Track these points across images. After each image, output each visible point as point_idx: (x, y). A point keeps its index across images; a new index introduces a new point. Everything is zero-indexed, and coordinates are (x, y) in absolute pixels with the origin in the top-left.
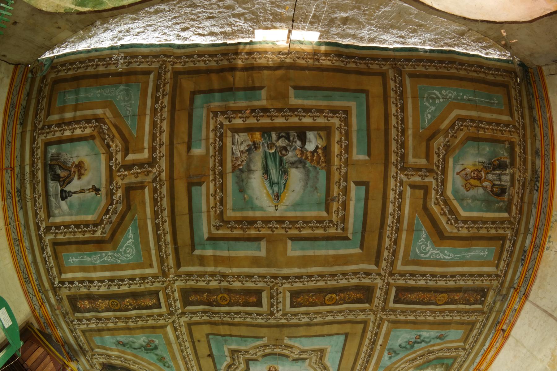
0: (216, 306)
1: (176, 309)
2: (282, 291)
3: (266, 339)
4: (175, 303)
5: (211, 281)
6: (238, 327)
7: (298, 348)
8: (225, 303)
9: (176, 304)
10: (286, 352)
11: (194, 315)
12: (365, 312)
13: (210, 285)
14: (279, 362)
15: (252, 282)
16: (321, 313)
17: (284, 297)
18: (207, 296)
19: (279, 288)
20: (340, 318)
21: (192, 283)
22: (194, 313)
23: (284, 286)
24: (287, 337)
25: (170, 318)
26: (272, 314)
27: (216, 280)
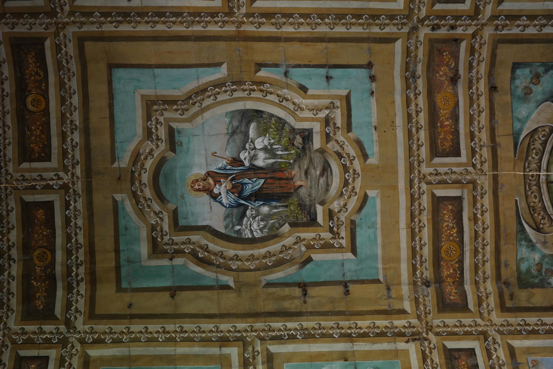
0: (54, 268)
1: (57, 333)
2: (20, 174)
3: (118, 197)
4: (45, 333)
5: (9, 273)
6: (96, 240)
7: (141, 143)
8: (49, 254)
9: (48, 331)
10: (149, 164)
11: (72, 305)
12: (60, 44)
13: (15, 275)
14: (178, 175)
15: (8, 215)
16: (63, 115)
17: (31, 170)
18: (35, 279)
19: (14, 178)
20: (74, 84)
21: (14, 301)
22: (68, 305)
23: (11, 170)
24: (113, 162)
25: (73, 346)
26: (65, 187)
27: (10, 265)
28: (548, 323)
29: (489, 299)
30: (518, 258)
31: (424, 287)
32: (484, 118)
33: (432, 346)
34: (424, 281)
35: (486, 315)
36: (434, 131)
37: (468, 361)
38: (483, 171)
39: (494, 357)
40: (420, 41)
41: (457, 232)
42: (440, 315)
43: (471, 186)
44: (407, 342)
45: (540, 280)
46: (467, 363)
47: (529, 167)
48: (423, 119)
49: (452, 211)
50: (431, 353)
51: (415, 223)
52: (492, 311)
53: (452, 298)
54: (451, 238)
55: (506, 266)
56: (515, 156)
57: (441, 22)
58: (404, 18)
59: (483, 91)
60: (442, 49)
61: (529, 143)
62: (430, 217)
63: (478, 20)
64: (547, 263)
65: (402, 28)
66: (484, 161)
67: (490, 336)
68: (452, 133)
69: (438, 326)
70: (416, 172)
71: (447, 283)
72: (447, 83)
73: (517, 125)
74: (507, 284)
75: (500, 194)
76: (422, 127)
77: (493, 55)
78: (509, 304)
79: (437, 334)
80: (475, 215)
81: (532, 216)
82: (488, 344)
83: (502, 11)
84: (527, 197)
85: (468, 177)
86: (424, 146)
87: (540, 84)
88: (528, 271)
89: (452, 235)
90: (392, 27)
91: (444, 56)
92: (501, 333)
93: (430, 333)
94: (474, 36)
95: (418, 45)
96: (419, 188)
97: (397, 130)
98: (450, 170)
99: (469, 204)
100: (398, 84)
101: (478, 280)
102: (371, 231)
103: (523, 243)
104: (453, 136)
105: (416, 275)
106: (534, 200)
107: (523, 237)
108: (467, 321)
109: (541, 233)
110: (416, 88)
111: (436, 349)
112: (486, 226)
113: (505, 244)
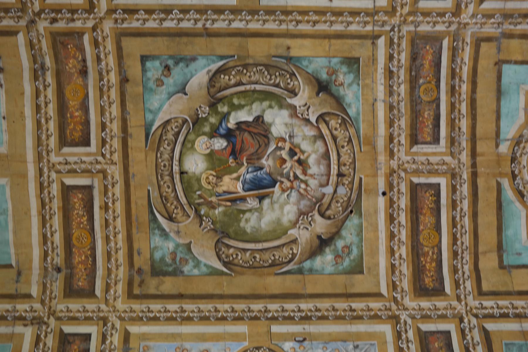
28: (171, 310)
29: (117, 286)
30: (152, 246)
31: (55, 273)
32: (115, 110)
33: (49, 330)
34: (55, 267)
35: (111, 301)
36: (64, 122)
37: (81, 346)
38: (113, 161)
39: (108, 342)
40: (41, 34)
41: (87, 220)
42: (66, 300)
43: (101, 175)
44: (25, 325)
45: (175, 268)
46: (79, 348)
47: (161, 157)
48: (52, 110)
49: (82, 199)
50: (46, 336)
51: (46, 210)
52: (118, 298)
53: (80, 284)
54: (81, 226)
55: (139, 254)
56: (146, 146)
57: (57, 15)
58: (18, 11)
59: (114, 83)
60: (64, 42)
61: (161, 135)
62: (61, 205)
63: (95, 14)
64: (181, 252)
65: (19, 21)
66: (114, 151)
67: (109, 321)
68: (81, 124)
69: (62, 311)
70: (45, 160)
71: (78, 270)
72: (76, 75)
73: (149, 117)
74: (140, 271)
75: (132, 183)
76: (51, 117)
77: (119, 49)
78: (137, 291)
79: (59, 319)
80: (106, 204)
81: (165, 205)
82: (106, 330)
83: (118, 5)
84: (159, 187)
85: (98, 167)
86: (53, 137)
87: (171, 76)
88: (162, 259)
89: (82, 223)
90: (9, 20)
91: (68, 49)
92: (121, 319)
93: (51, 317)
94: (94, 29)
95: (41, 38)
96: (49, 177)
97: (27, 121)
98: (80, 160)
99: (100, 193)
100: (27, 75)
101: (110, 266)
102: (1, 218)
103: (156, 231)
104: (83, 127)
105: (47, 260)
106: (167, 190)
107: (156, 226)
108: (91, 306)
109: (174, 222)
110: (45, 81)
111: (53, 333)
112: (116, 215)
113: (137, 233)
